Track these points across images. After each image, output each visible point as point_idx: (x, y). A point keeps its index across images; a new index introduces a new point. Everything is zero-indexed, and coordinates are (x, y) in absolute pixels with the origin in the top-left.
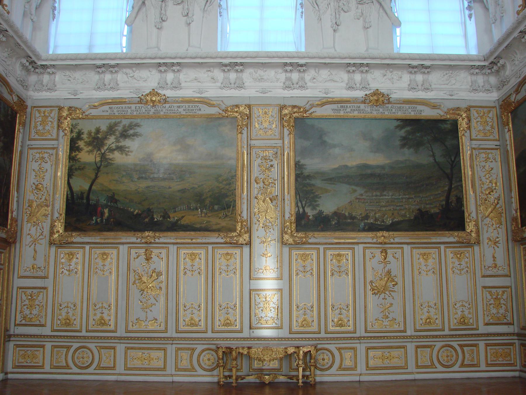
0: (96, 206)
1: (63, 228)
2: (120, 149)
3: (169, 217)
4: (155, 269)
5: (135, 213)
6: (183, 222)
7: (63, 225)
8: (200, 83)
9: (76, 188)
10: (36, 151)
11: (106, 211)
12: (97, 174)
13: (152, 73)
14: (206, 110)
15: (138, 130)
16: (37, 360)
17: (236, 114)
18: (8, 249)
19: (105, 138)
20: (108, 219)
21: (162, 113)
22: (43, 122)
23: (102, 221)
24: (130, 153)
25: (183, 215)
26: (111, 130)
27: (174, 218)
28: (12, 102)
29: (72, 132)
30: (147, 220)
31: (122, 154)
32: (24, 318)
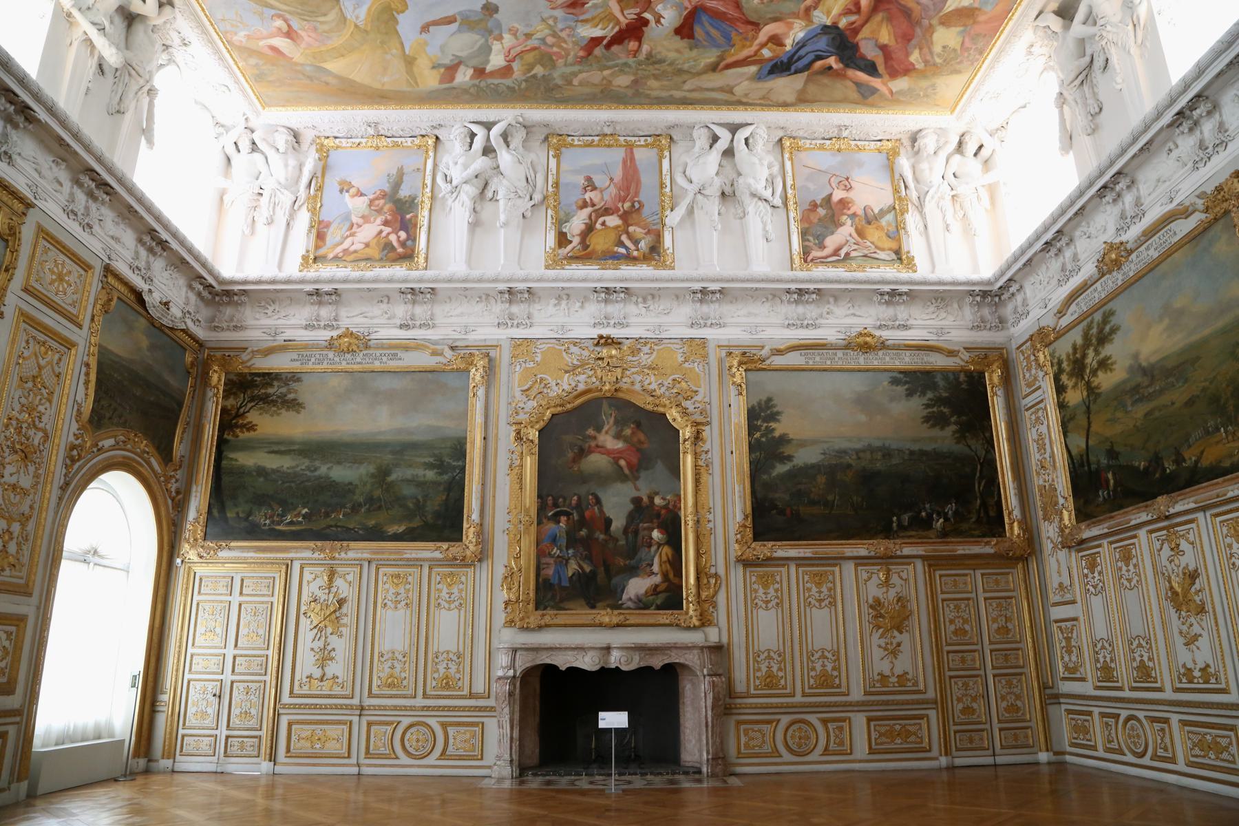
0: (1098, 471)
1: (1073, 516)
2: (1104, 364)
3: (1184, 460)
4: (1187, 565)
5: (1142, 467)
6: (1205, 463)
7: (1073, 512)
8: (1167, 183)
9: (1074, 452)
10: (1030, 412)
11: (1110, 476)
12: (1089, 418)
13: (1108, 212)
14: (1183, 227)
15: (1114, 321)
16: (1088, 737)
17: (1225, 205)
18: (1020, 566)
19: (1084, 356)
20: (1115, 490)
21: (1131, 274)
22: (1029, 370)
23: (1108, 493)
24: (1114, 367)
25: (1202, 448)
26: (1086, 336)
27: (1190, 459)
28: (963, 364)
29: (1052, 366)
30: (1157, 475)
31: (1106, 372)
32: (1066, 668)
